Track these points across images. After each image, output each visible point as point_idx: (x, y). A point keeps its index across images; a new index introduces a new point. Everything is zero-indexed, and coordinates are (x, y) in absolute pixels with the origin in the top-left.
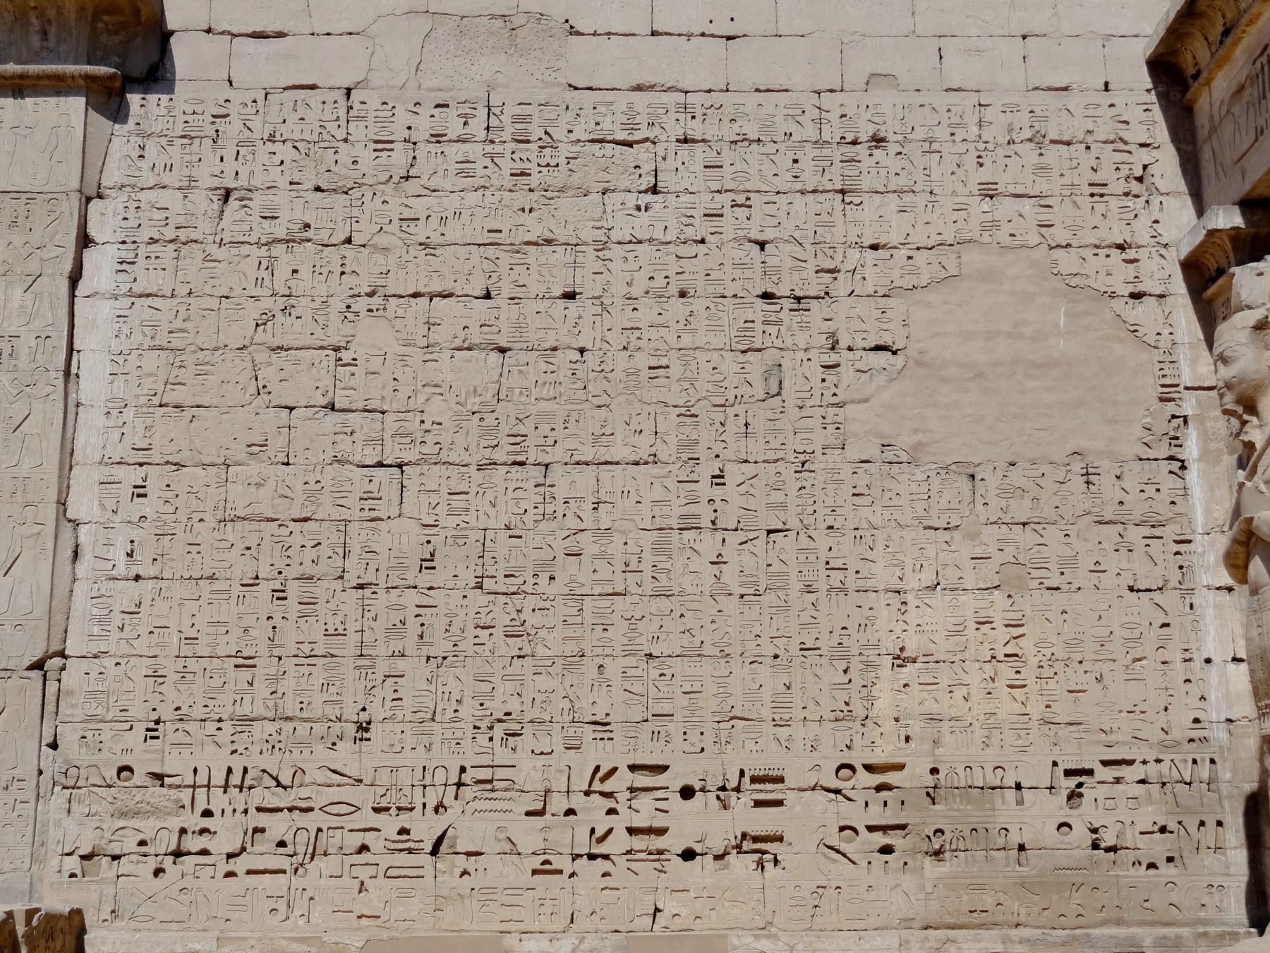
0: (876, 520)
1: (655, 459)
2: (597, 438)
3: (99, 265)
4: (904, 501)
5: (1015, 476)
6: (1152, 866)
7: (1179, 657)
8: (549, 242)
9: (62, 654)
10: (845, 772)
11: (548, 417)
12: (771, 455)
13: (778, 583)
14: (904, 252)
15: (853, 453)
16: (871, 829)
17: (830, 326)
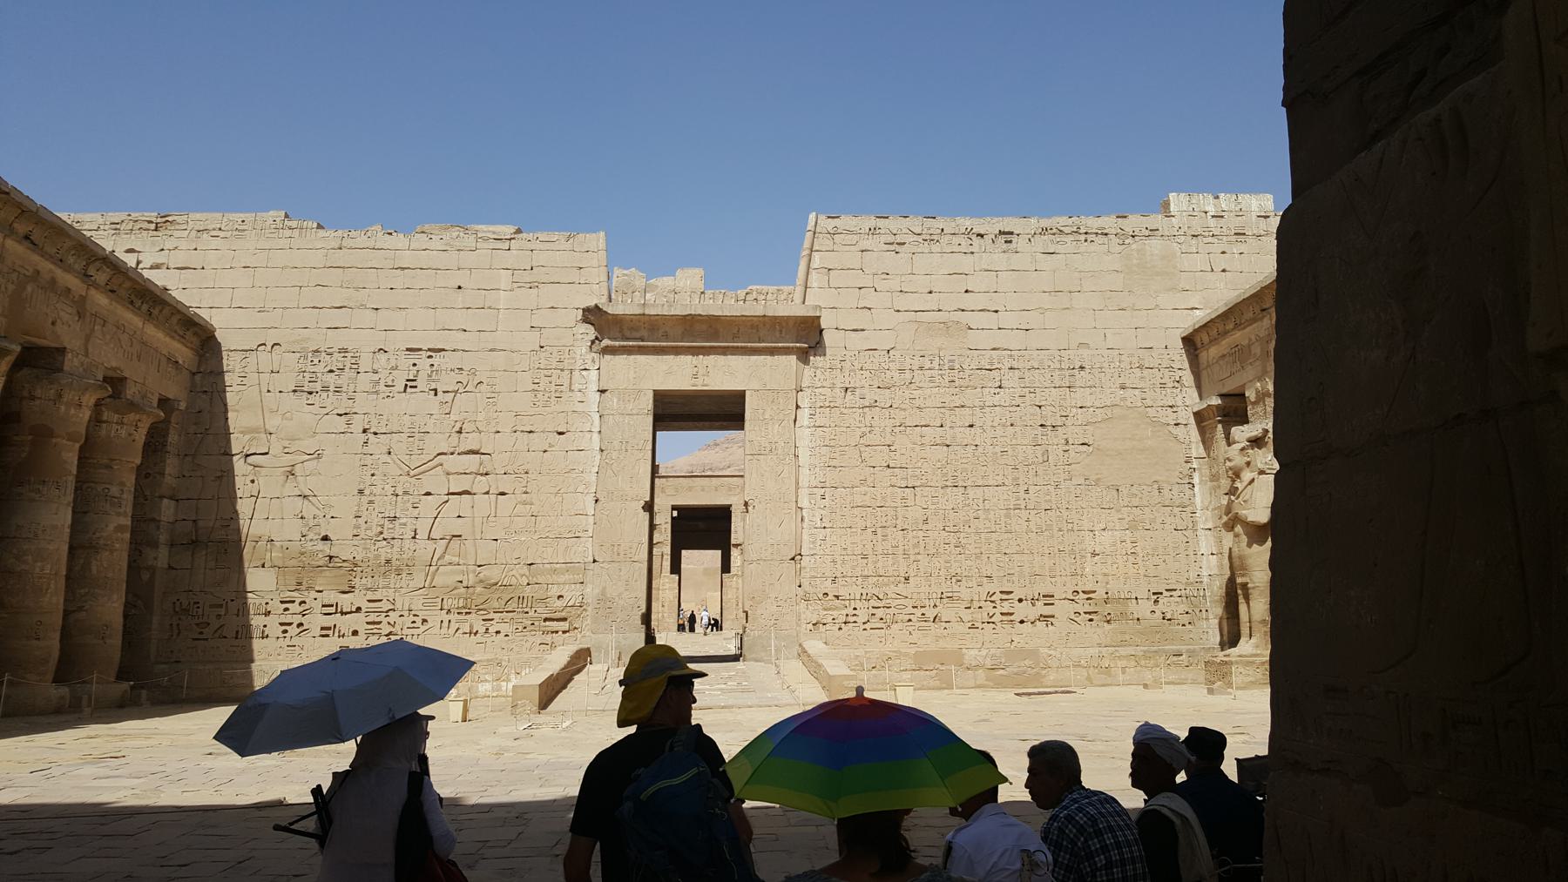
0: (1084, 506)
1: (1004, 484)
2: (983, 477)
3: (804, 415)
4: (1094, 499)
5: (1134, 490)
6: (1183, 625)
7: (1192, 553)
8: (963, 406)
9: (800, 554)
10: (1075, 594)
11: (965, 470)
12: (1045, 483)
13: (1049, 528)
14: (1092, 409)
15: (1075, 482)
16: (1085, 613)
17: (1065, 436)
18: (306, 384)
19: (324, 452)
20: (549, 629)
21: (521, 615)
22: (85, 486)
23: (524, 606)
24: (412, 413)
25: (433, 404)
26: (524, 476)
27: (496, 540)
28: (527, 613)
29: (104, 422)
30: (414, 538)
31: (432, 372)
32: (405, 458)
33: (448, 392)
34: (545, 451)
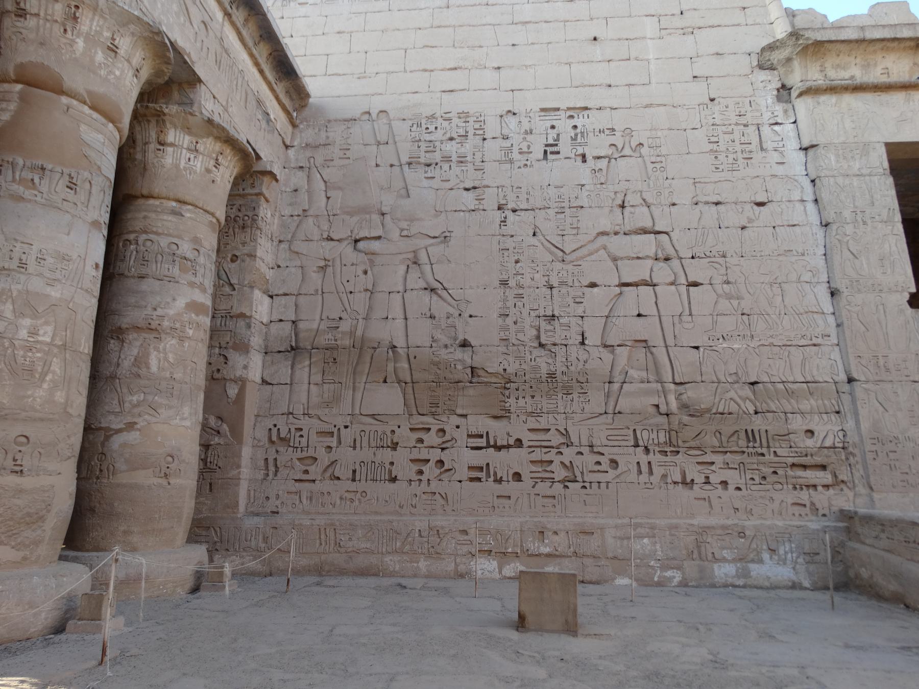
18: (422, 154)
19: (452, 234)
20: (800, 481)
21: (755, 459)
22: (143, 237)
23: (757, 445)
24: (559, 184)
25: (584, 173)
26: (721, 260)
27: (697, 348)
28: (763, 455)
29: (172, 145)
30: (583, 343)
31: (576, 135)
32: (556, 240)
33: (599, 158)
34: (743, 228)
